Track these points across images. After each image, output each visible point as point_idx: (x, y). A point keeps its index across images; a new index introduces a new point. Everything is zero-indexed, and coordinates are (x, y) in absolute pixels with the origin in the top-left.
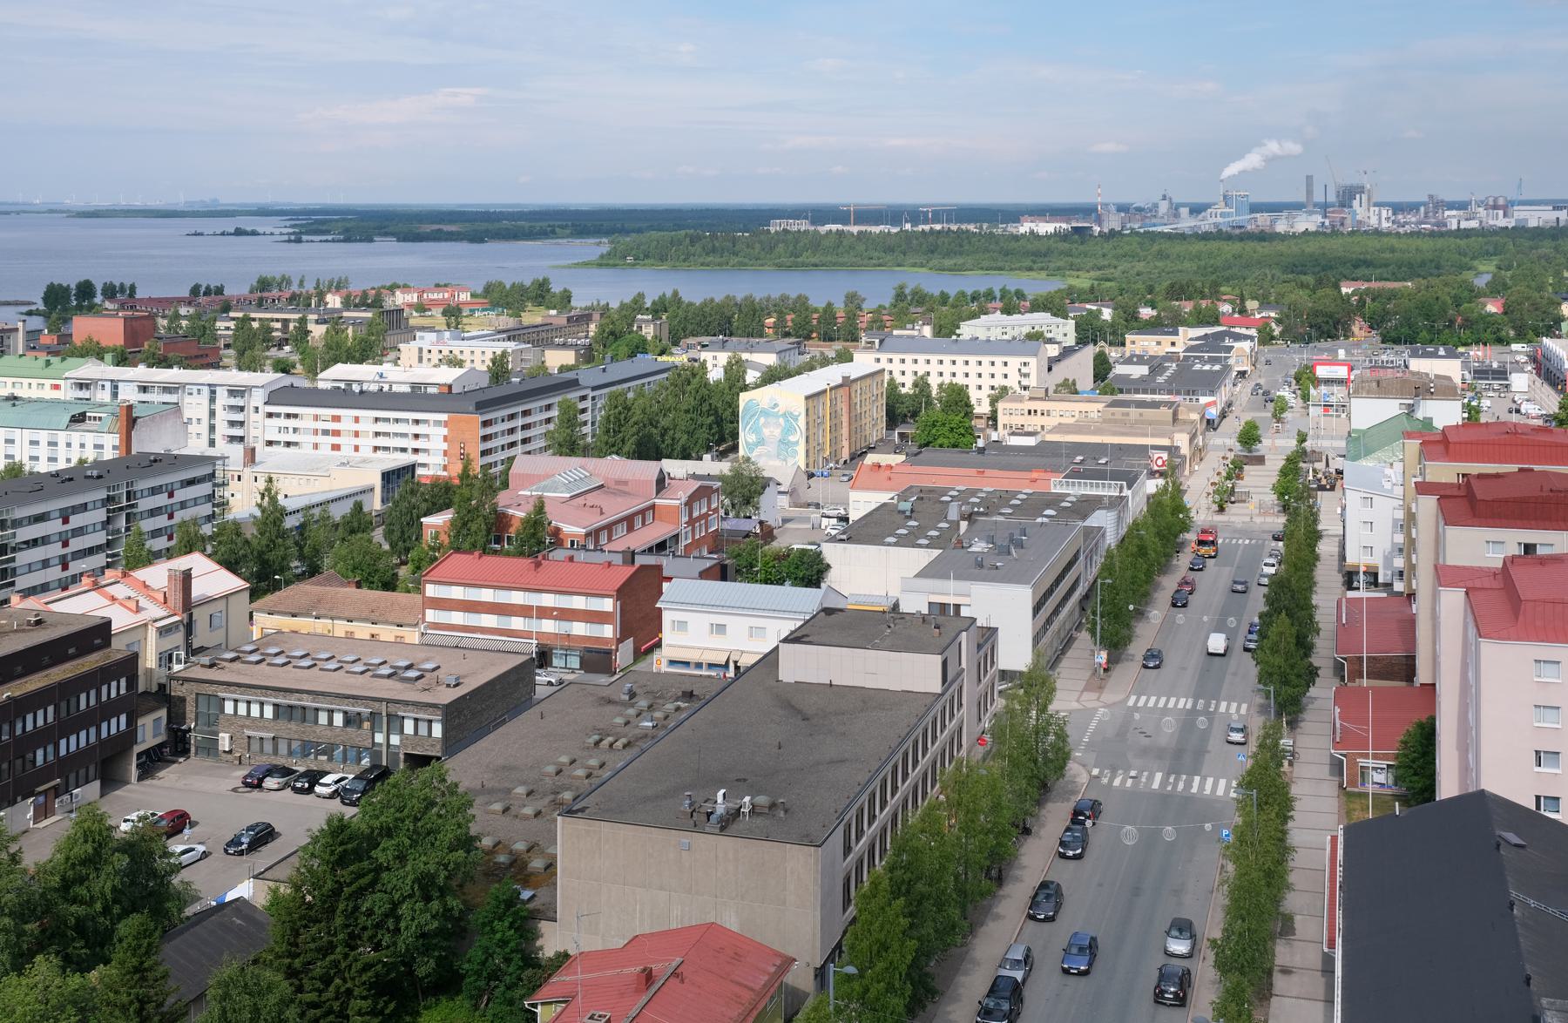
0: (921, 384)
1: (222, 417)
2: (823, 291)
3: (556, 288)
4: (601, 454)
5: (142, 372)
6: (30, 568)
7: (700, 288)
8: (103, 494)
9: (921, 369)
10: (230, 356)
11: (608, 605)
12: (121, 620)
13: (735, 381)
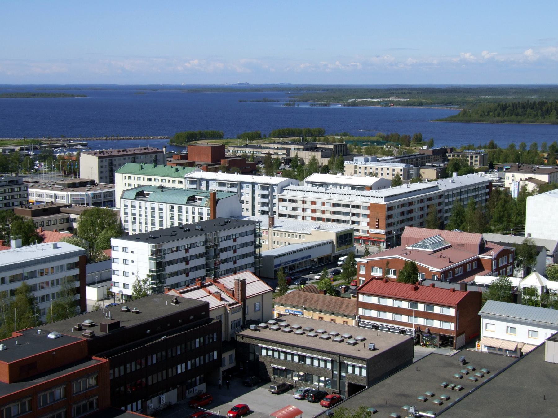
1: (258, 199)
6: (172, 275)
11: (452, 312)
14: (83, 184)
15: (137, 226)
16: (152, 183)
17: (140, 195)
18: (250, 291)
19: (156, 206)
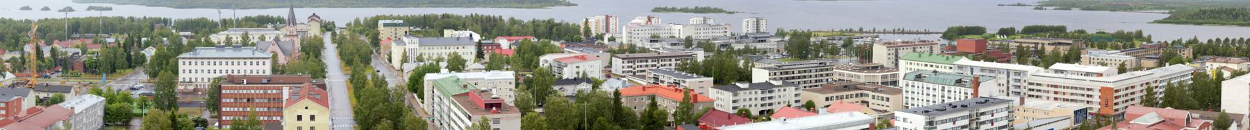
1: (1012, 82)
3: (1145, 35)
4: (1163, 106)
5: (982, 64)
7: (1206, 34)
8: (967, 113)
10: (1014, 58)
13: (1220, 78)
14: (875, 68)
15: (915, 102)
16: (929, 68)
17: (919, 77)
19: (931, 86)
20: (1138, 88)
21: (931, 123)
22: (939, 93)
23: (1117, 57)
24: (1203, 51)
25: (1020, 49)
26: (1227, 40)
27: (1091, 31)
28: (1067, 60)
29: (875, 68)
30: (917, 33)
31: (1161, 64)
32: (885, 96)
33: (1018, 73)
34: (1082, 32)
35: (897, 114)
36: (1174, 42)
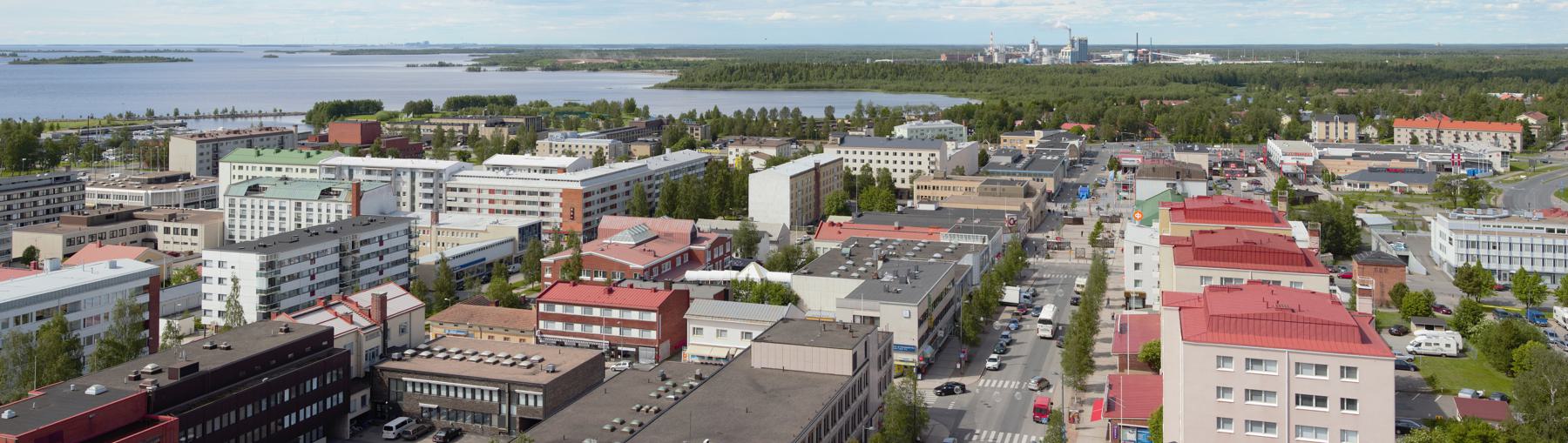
0: (867, 169)
1: (419, 190)
2: (811, 105)
3: (640, 105)
5: (369, 161)
7: (732, 103)
8: (336, 243)
9: (867, 157)
12: (340, 327)
16: (274, 174)
18: (392, 309)
20: (621, 189)
21: (270, 265)
22: (290, 214)
23: (590, 142)
24: (719, 129)
25: (440, 133)
26: (764, 110)
27: (556, 102)
28: (514, 149)
29: (173, 179)
30: (260, 115)
31: (658, 150)
32: (189, 226)
33: (428, 173)
34: (544, 104)
35: (207, 255)
36: (683, 116)
